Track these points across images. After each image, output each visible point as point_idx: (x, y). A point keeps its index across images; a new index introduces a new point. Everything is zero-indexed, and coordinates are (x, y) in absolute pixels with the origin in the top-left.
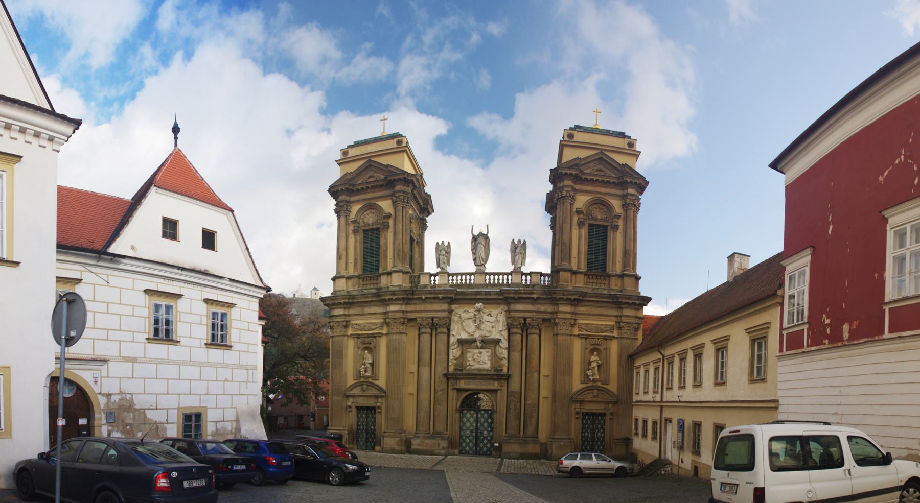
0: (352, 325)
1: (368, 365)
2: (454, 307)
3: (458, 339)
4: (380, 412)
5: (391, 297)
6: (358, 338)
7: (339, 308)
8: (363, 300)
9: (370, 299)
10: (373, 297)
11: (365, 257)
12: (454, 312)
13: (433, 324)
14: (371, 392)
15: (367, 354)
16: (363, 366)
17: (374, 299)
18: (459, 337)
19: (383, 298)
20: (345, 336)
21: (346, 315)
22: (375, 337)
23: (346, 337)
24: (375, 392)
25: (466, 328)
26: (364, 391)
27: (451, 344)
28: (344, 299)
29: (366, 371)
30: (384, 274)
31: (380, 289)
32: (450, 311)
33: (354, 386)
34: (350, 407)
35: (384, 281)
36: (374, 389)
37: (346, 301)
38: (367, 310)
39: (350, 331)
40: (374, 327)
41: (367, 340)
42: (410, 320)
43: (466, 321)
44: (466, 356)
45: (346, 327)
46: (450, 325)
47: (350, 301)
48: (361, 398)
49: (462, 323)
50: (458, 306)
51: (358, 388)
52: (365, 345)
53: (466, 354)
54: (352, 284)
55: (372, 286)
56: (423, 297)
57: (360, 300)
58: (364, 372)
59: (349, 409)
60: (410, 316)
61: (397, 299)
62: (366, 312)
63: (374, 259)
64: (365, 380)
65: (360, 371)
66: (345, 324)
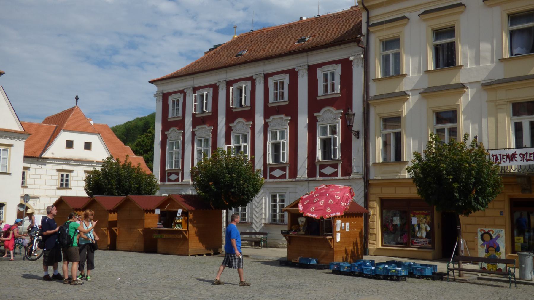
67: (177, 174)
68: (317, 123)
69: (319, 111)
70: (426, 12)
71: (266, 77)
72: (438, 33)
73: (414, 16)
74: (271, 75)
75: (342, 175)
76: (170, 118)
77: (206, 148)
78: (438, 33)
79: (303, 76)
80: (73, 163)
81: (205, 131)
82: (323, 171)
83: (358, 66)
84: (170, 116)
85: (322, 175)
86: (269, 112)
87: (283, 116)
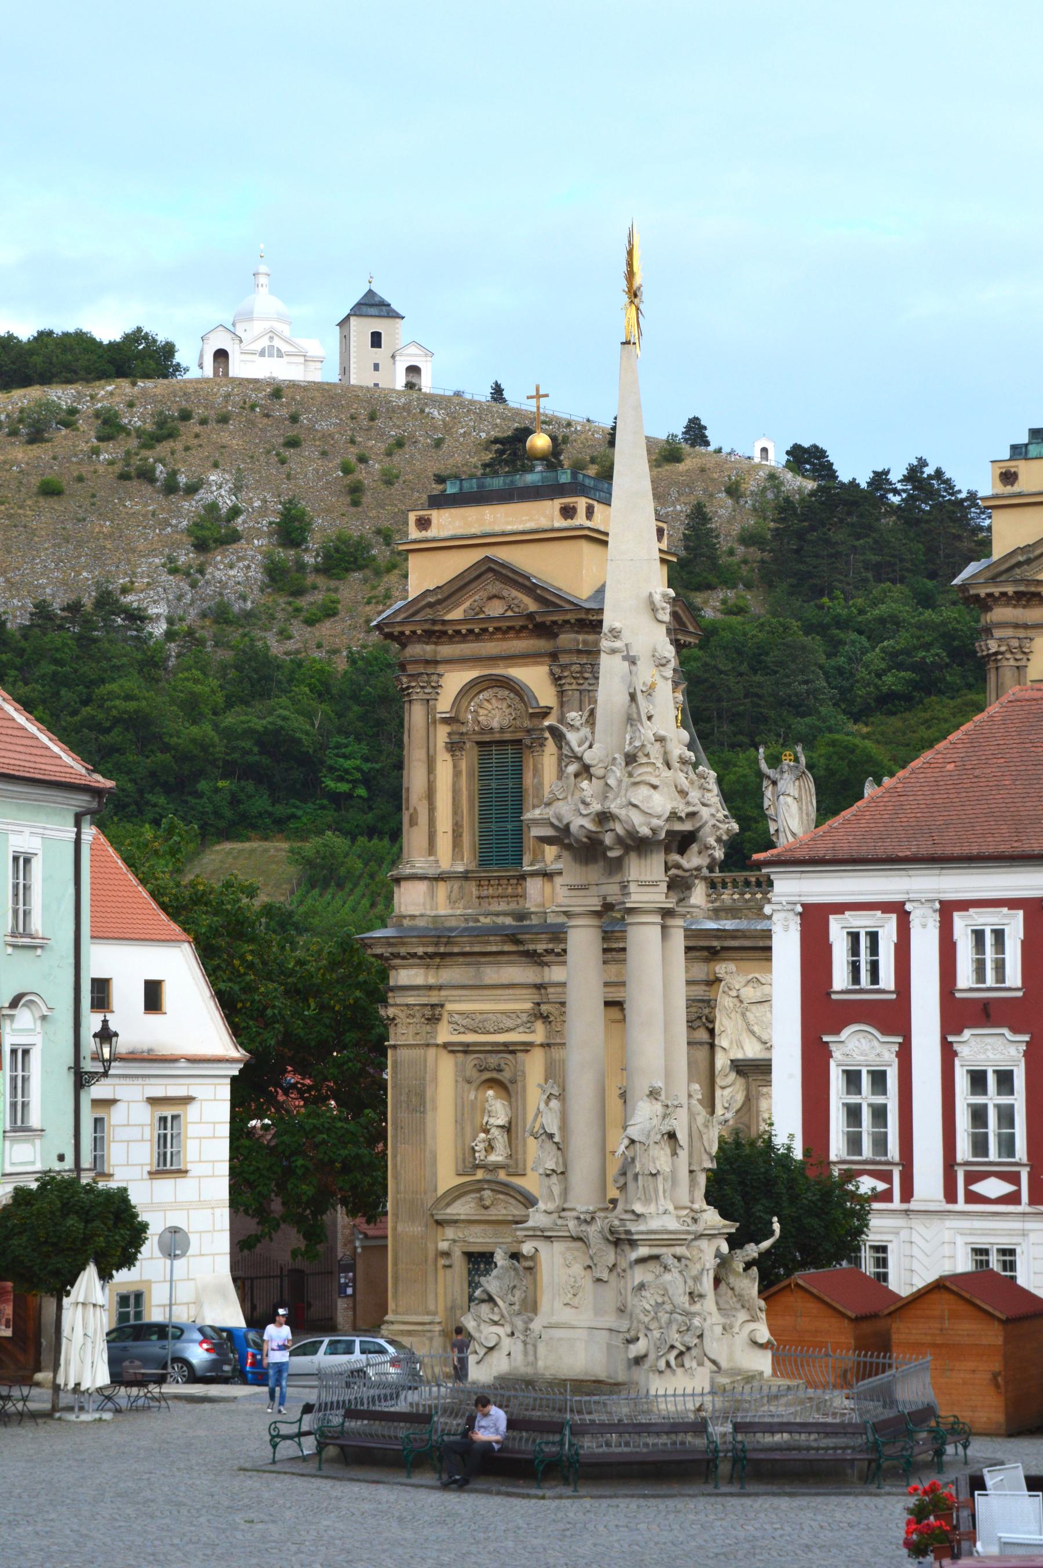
0: (450, 1014)
1: (495, 1132)
2: (721, 968)
3: (732, 1061)
4: (530, 1269)
5: (550, 946)
6: (465, 1052)
7: (411, 966)
8: (477, 949)
9: (494, 949)
10: (504, 942)
12: (723, 983)
14: (504, 1212)
15: (491, 1102)
16: (482, 1135)
17: (507, 948)
18: (740, 1056)
19: (531, 947)
20: (428, 1045)
21: (430, 988)
22: (513, 1052)
23: (432, 1052)
24: (516, 1212)
25: (756, 1029)
26: (486, 1208)
28: (424, 945)
30: (534, 874)
31: (521, 916)
33: (456, 1194)
34: (446, 1254)
35: (534, 888)
36: (512, 1201)
37: (430, 950)
38: (492, 974)
39: (444, 1034)
40: (509, 1023)
41: (493, 1060)
43: (754, 1008)
44: (757, 1107)
45: (434, 1020)
47: (442, 950)
48: (477, 1229)
49: (743, 1015)
50: (731, 966)
51: (468, 1198)
52: (487, 1075)
53: (758, 1099)
54: (449, 897)
55: (503, 907)
57: (467, 949)
58: (484, 1152)
59: (442, 1262)
62: (488, 981)
64: (489, 1177)
65: (474, 1151)
66: (428, 1012)
67: (886, 1177)
76: (842, 992)
77: (1005, 1100)
84: (840, 979)
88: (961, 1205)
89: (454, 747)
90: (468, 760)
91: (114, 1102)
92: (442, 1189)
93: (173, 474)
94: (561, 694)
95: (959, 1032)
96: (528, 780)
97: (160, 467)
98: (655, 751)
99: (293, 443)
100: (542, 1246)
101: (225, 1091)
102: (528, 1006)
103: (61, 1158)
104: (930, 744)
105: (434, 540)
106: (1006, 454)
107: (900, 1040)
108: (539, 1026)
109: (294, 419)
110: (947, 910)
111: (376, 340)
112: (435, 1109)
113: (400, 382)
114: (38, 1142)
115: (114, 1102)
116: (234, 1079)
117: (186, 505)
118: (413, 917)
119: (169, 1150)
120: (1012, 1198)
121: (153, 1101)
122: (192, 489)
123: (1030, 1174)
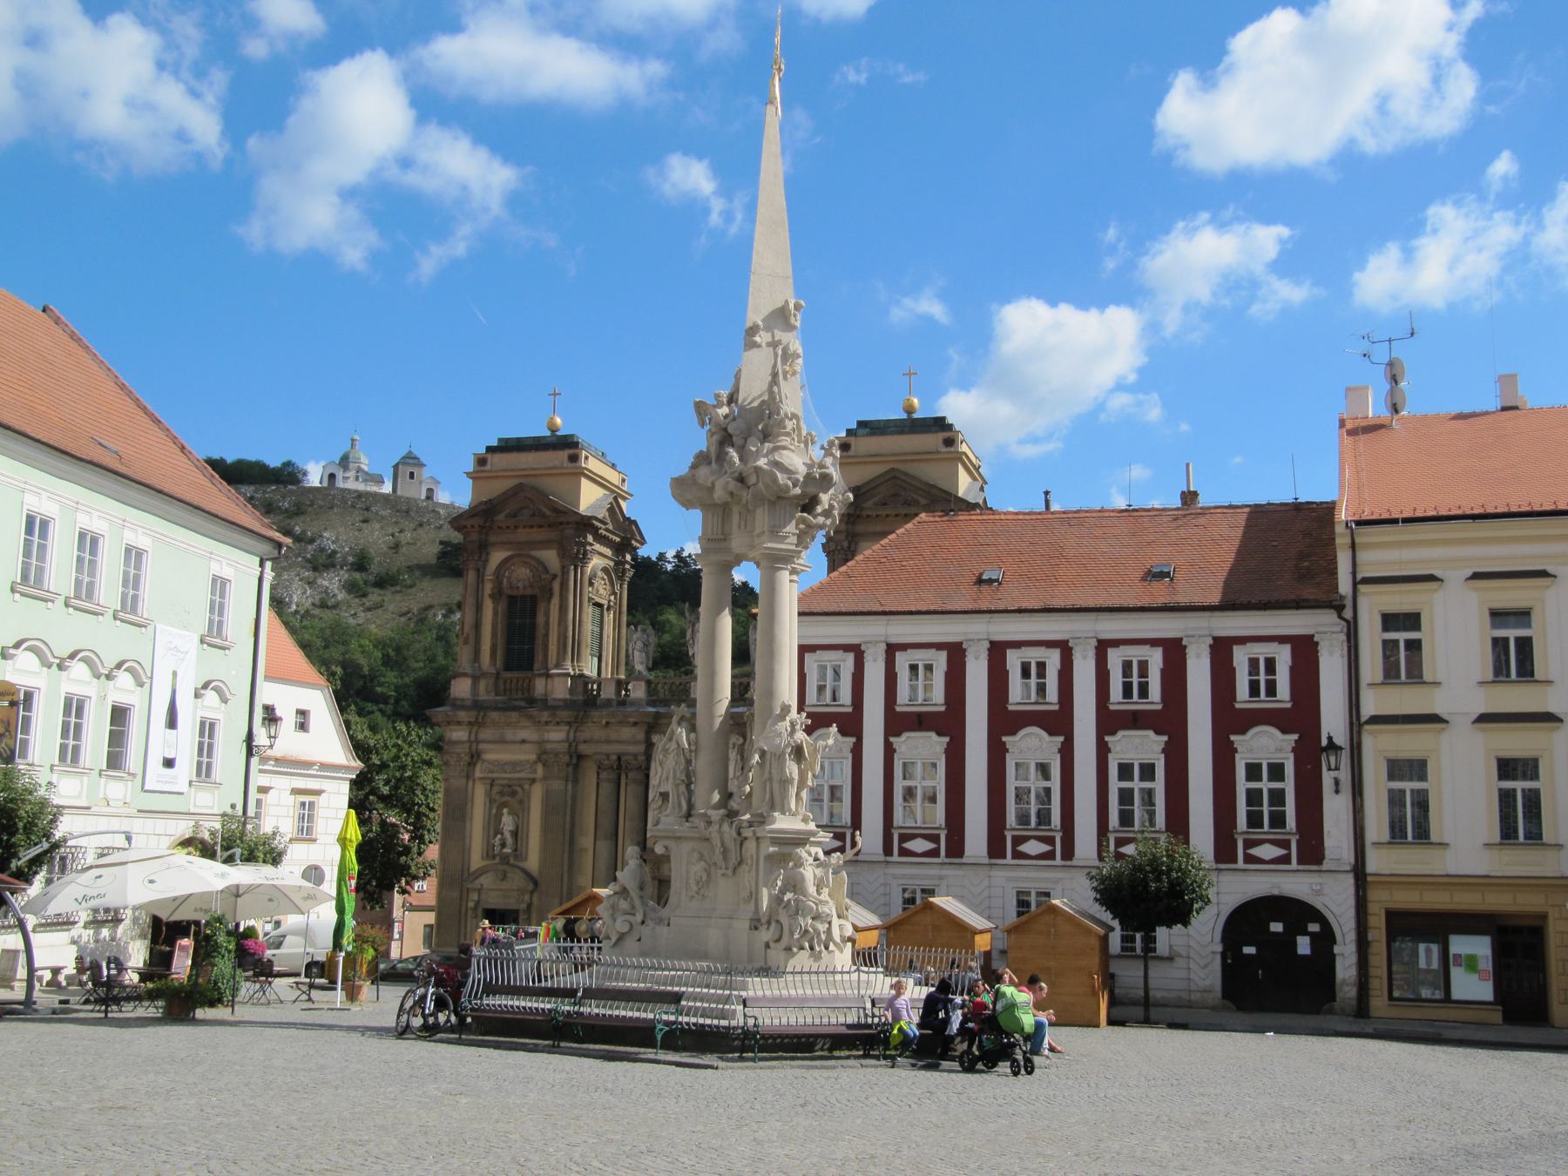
0: (484, 761)
1: (508, 836)
11: (509, 641)
13: (619, 767)
27: (650, 799)
29: (503, 845)
30: (540, 675)
32: (650, 746)
33: (482, 872)
39: (478, 774)
42: (580, 757)
46: (648, 768)
56: (604, 722)
60: (583, 748)
61: (558, 723)
63: (526, 647)
68: (1237, 756)
69: (1243, 732)
70: (1477, 576)
71: (1103, 647)
72: (1499, 616)
73: (1456, 577)
74: (1116, 643)
75: (1300, 862)
78: (1499, 616)
79: (1198, 656)
80: (271, 768)
81: (925, 748)
82: (1255, 851)
83: (1331, 653)
85: (1250, 859)
86: (1109, 722)
87: (1151, 733)
88: (896, 857)
89: (497, 595)
90: (502, 607)
91: (271, 788)
92: (473, 869)
93: (304, 532)
94: (563, 568)
95: (898, 735)
96: (540, 619)
97: (297, 528)
98: (790, 425)
99: (365, 521)
100: (671, 844)
101: (345, 788)
102: (533, 757)
103: (233, 806)
104: (885, 534)
105: (488, 471)
106: (843, 434)
107: (853, 740)
108: (540, 769)
109: (367, 509)
110: (892, 649)
111: (412, 475)
112: (471, 819)
113: (423, 497)
114: (216, 792)
115: (271, 788)
116: (351, 780)
117: (310, 547)
118: (463, 700)
119: (306, 825)
120: (934, 853)
121: (295, 791)
122: (312, 541)
123: (947, 836)
